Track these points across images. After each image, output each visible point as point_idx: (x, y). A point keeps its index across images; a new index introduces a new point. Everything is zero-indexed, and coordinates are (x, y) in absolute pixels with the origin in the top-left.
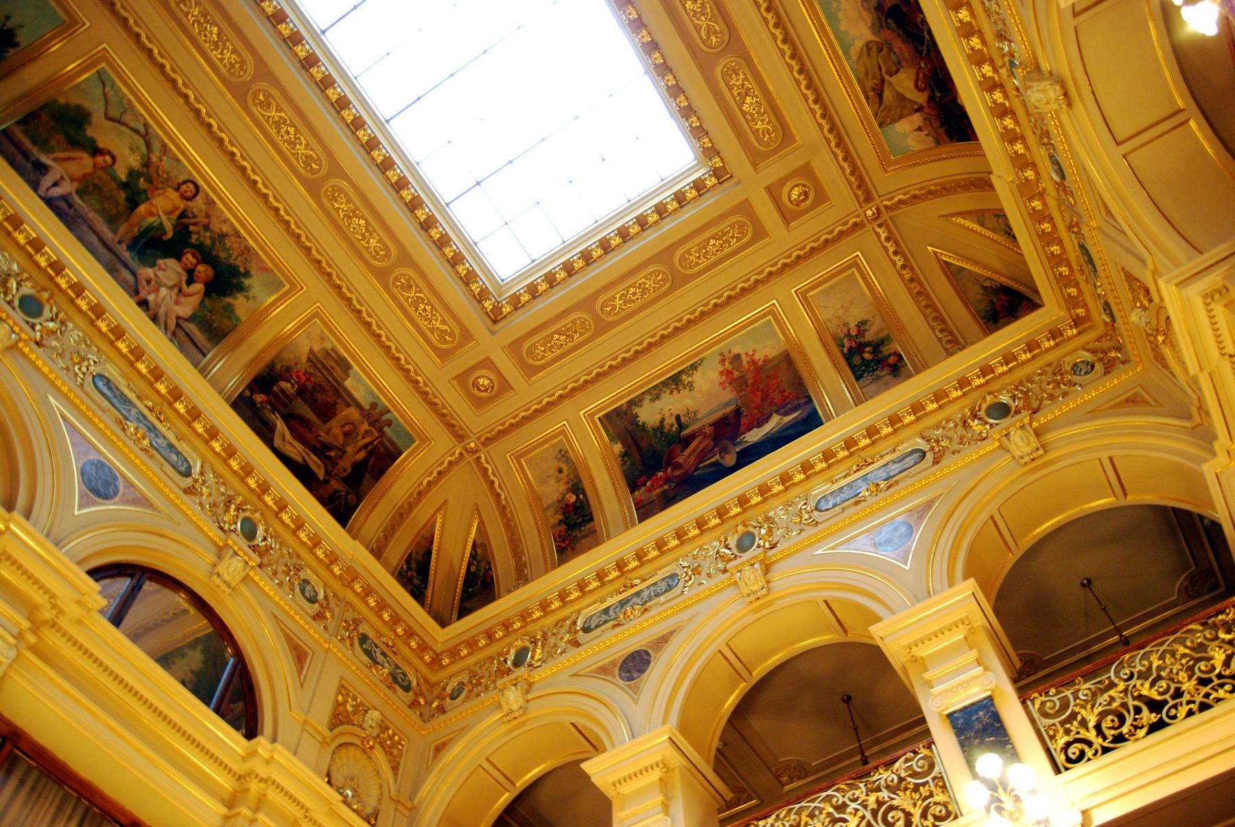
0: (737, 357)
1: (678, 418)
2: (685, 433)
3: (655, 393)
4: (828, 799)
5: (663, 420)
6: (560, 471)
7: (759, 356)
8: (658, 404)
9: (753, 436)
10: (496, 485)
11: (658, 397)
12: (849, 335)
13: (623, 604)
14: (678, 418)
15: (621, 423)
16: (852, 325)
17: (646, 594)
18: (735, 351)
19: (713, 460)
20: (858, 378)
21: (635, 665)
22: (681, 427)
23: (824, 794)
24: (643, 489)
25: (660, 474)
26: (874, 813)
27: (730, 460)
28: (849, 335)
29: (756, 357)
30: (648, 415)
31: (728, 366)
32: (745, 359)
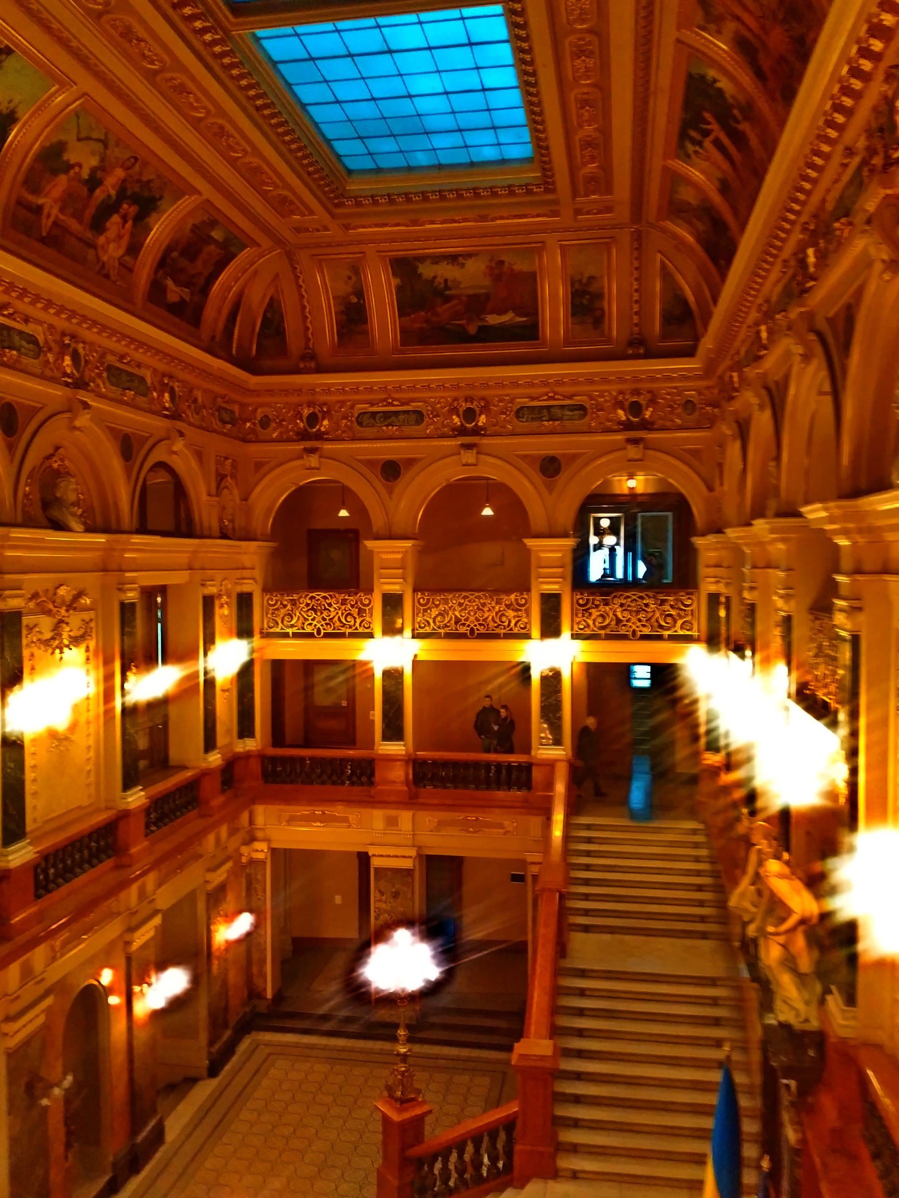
0: (502, 262)
1: (446, 281)
2: (447, 293)
3: (437, 259)
4: (479, 598)
5: (435, 277)
6: (350, 278)
7: (517, 267)
8: (435, 267)
9: (493, 320)
10: (307, 310)
11: (437, 263)
12: (580, 281)
13: (387, 415)
14: (446, 281)
15: (404, 267)
16: (586, 275)
17: (402, 417)
18: (502, 258)
19: (461, 322)
20: (573, 315)
21: (391, 471)
22: (447, 287)
23: (477, 594)
24: (408, 318)
25: (422, 313)
26: (497, 613)
27: (472, 330)
28: (580, 281)
29: (515, 267)
30: (426, 270)
31: (493, 264)
32: (506, 264)
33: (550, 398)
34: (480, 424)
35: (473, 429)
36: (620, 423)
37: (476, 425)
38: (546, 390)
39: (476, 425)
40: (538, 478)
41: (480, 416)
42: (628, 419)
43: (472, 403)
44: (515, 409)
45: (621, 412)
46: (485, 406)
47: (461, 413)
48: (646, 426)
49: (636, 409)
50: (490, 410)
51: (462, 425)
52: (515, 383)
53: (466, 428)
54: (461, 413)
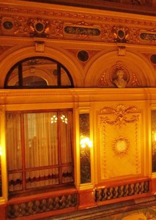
33: (82, 24)
34: (46, 32)
35: (42, 34)
36: (115, 39)
37: (44, 32)
38: (79, 20)
39: (44, 32)
40: (77, 60)
41: (45, 28)
42: (118, 38)
43: (41, 21)
44: (64, 27)
45: (115, 34)
46: (48, 24)
47: (35, 25)
48: (125, 41)
49: (121, 33)
50: (50, 26)
51: (35, 31)
52: (62, 15)
53: (37, 33)
54: (35, 25)
